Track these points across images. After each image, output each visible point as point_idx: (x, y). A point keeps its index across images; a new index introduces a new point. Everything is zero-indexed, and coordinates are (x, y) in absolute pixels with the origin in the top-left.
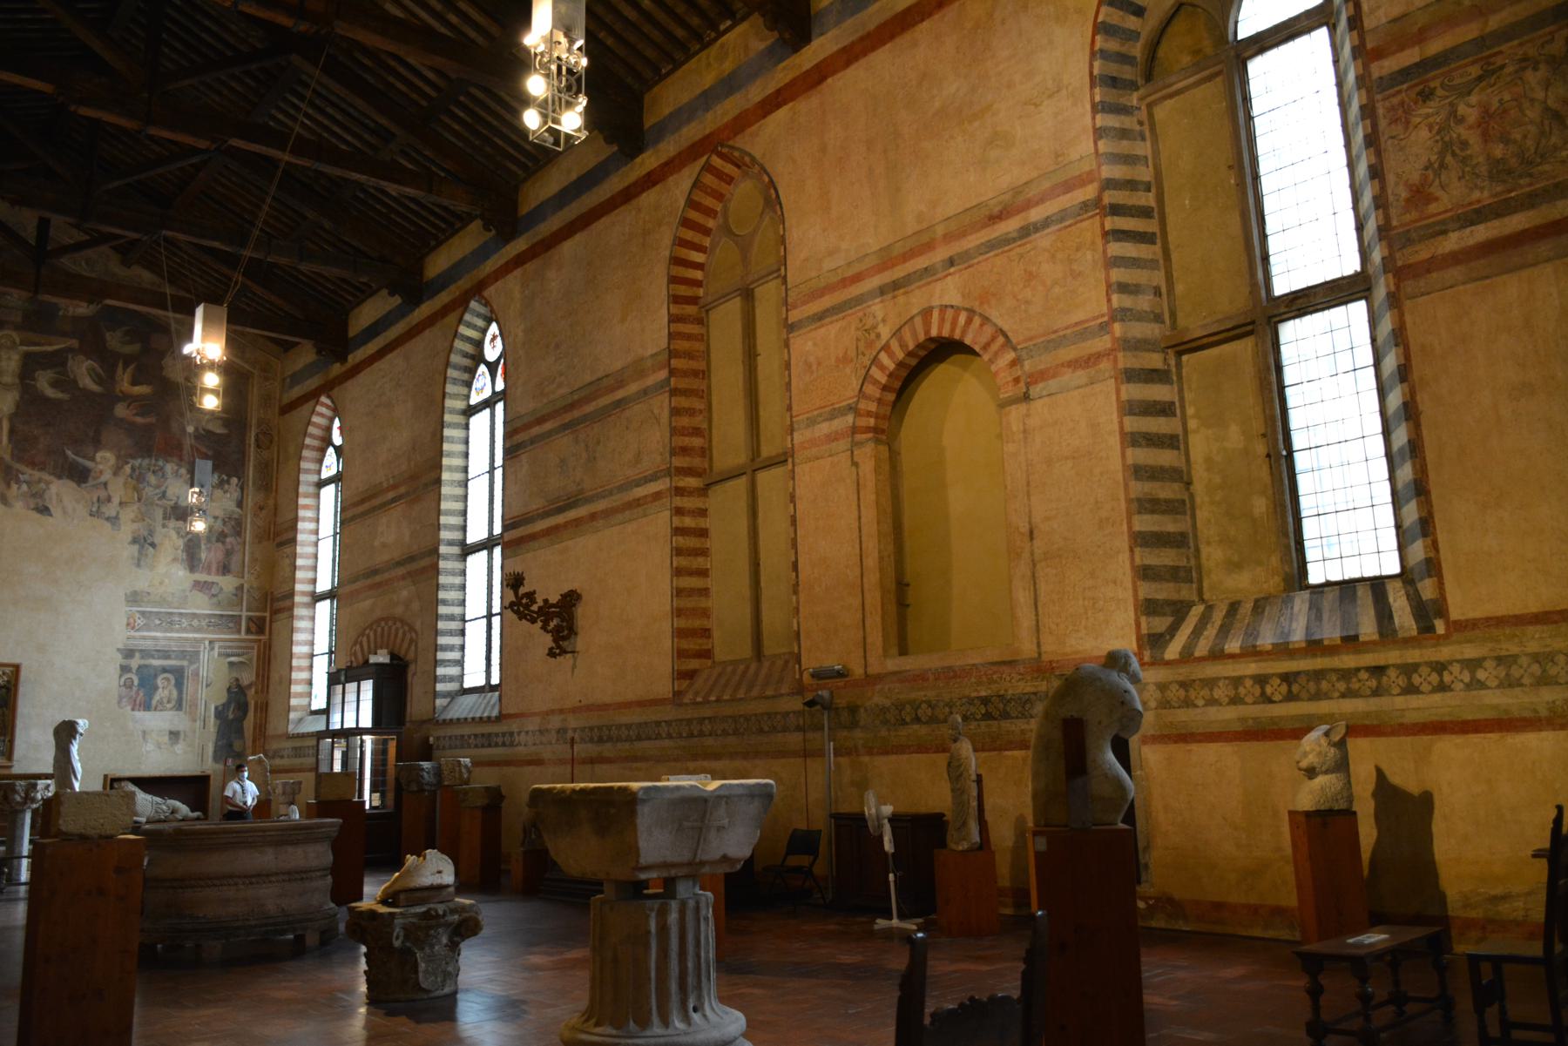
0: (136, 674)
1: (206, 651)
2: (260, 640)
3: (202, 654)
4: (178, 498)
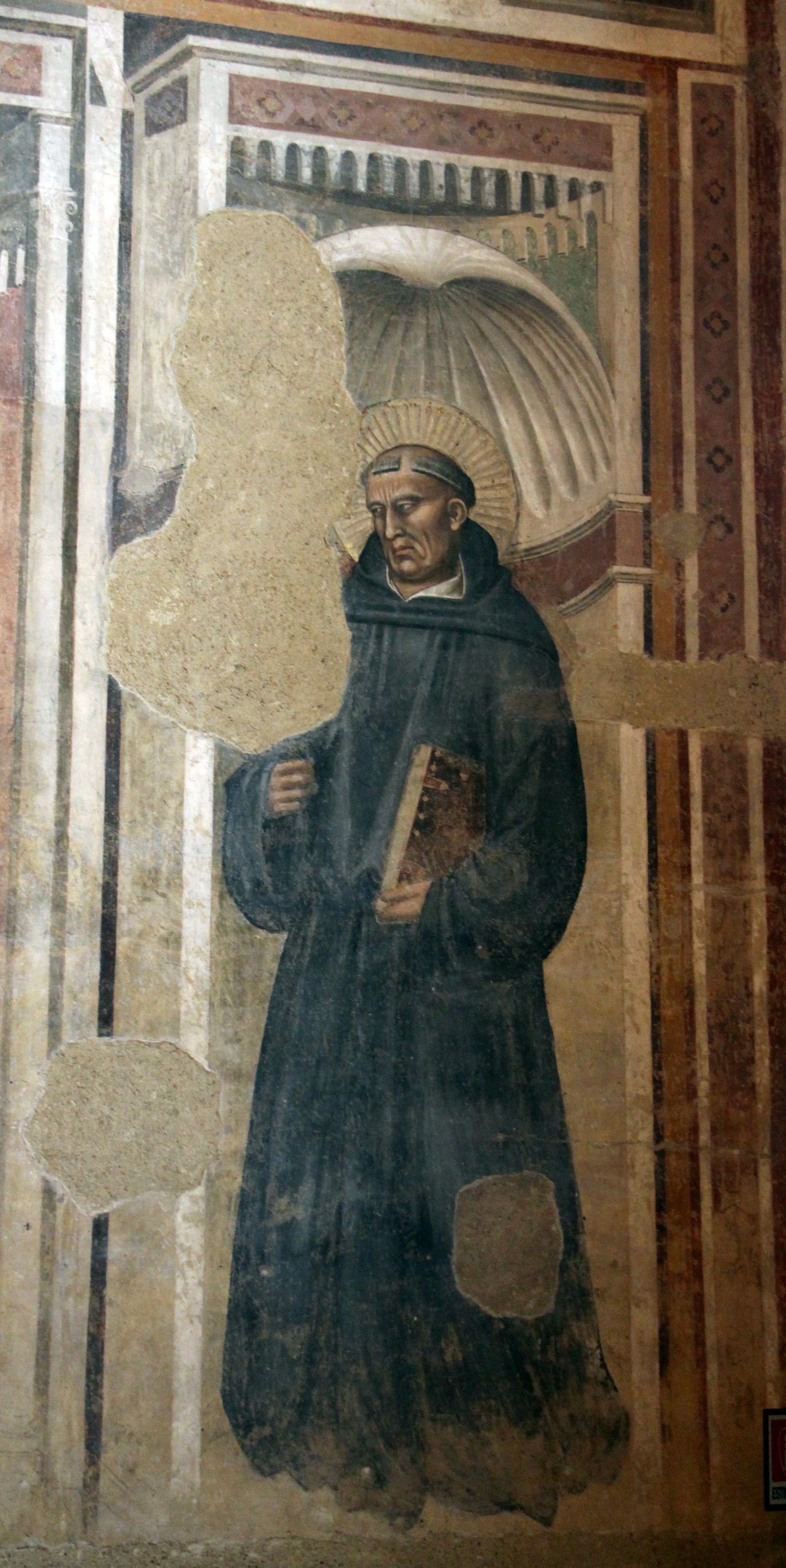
2: (671, 66)
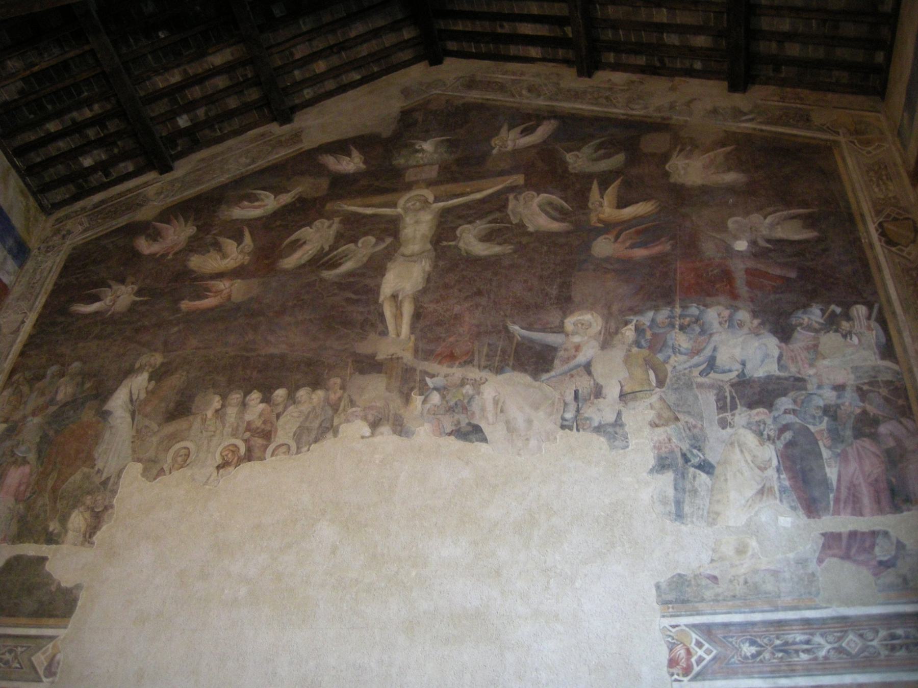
4: (743, 364)
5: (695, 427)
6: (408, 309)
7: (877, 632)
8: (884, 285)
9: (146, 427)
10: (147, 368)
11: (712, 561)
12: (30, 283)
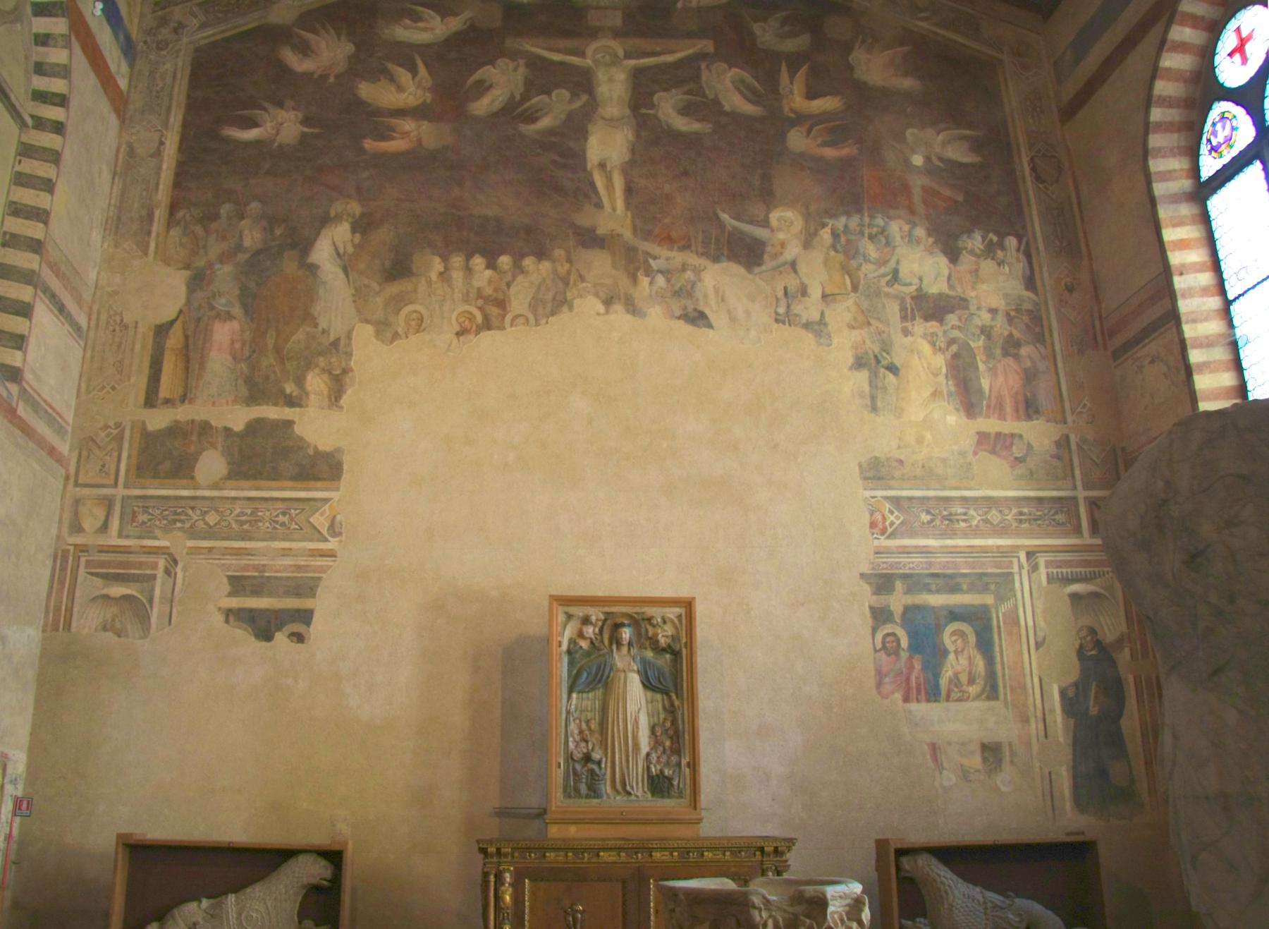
0: (902, 626)
1: (1025, 572)
3: (1017, 577)
4: (921, 279)
5: (883, 332)
6: (619, 182)
7: (1011, 510)
8: (1032, 219)
9: (365, 285)
10: (345, 217)
11: (899, 448)
12: (151, 92)
